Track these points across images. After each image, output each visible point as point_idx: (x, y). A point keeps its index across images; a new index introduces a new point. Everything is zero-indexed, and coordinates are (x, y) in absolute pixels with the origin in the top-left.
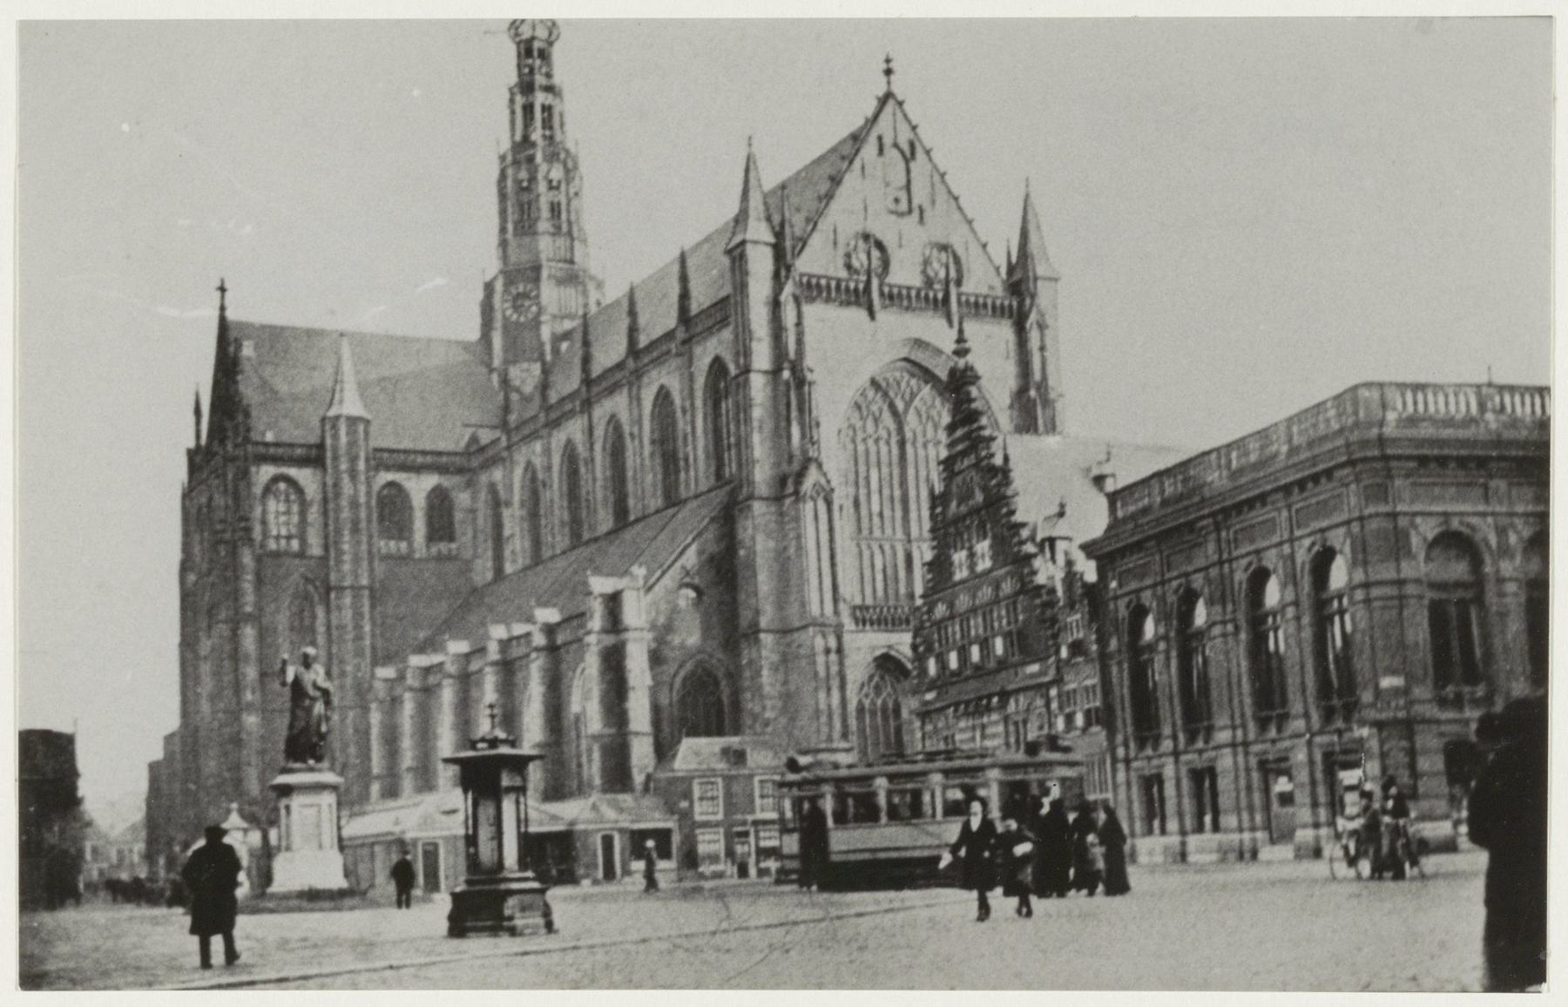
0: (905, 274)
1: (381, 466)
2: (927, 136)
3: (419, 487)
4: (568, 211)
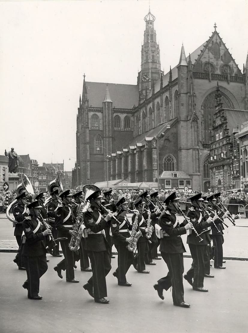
0: (218, 72)
1: (115, 112)
2: (224, 41)
3: (122, 116)
4: (156, 57)
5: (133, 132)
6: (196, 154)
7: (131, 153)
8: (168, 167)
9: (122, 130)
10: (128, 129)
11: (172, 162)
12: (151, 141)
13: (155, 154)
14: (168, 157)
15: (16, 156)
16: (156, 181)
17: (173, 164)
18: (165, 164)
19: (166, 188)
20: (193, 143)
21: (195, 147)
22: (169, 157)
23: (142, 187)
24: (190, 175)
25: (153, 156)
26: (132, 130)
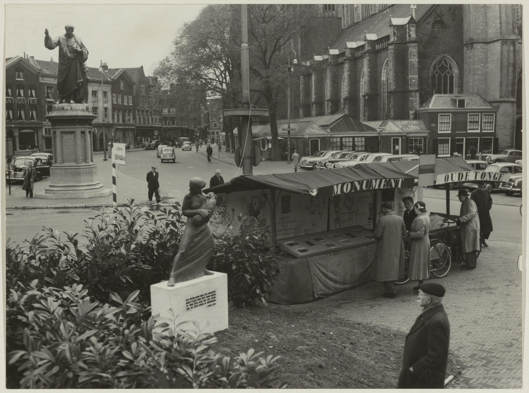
5: (341, 18)
6: (509, 51)
7: (350, 56)
8: (440, 84)
9: (319, 16)
10: (330, 14)
11: (448, 72)
12: (405, 25)
13: (414, 56)
14: (440, 62)
15: (79, 49)
16: (416, 117)
17: (452, 77)
18: (433, 77)
19: (439, 132)
20: (504, 25)
21: (507, 37)
22: (443, 62)
23: (387, 131)
24: (491, 103)
25: (410, 60)
26: (340, 15)
